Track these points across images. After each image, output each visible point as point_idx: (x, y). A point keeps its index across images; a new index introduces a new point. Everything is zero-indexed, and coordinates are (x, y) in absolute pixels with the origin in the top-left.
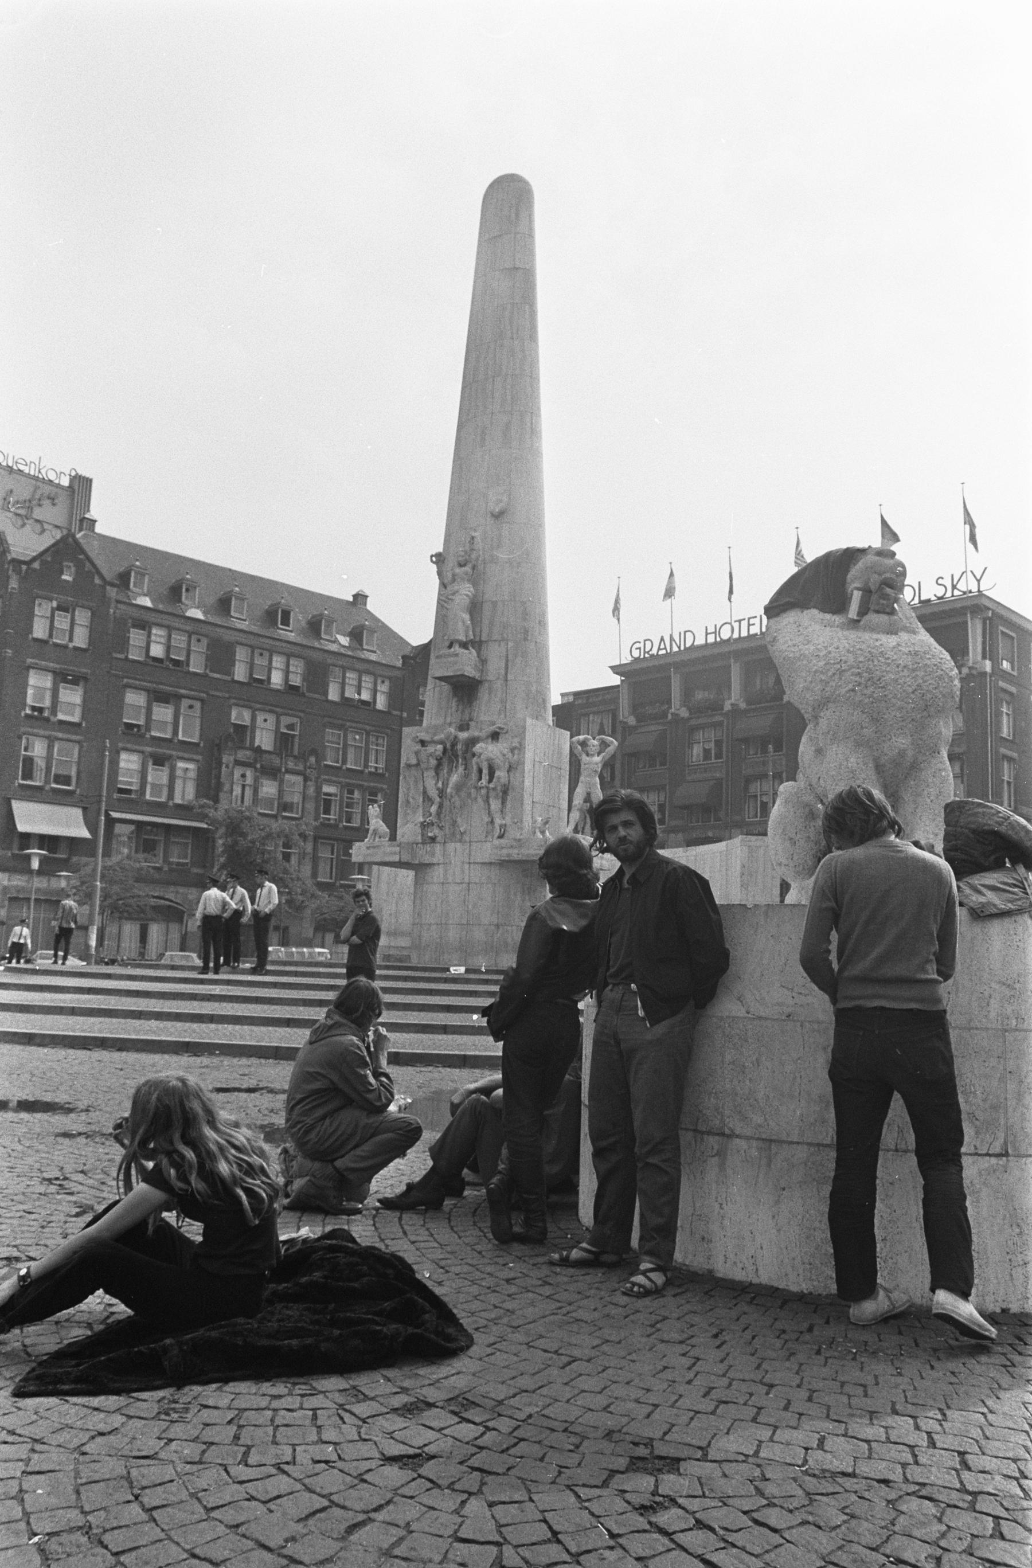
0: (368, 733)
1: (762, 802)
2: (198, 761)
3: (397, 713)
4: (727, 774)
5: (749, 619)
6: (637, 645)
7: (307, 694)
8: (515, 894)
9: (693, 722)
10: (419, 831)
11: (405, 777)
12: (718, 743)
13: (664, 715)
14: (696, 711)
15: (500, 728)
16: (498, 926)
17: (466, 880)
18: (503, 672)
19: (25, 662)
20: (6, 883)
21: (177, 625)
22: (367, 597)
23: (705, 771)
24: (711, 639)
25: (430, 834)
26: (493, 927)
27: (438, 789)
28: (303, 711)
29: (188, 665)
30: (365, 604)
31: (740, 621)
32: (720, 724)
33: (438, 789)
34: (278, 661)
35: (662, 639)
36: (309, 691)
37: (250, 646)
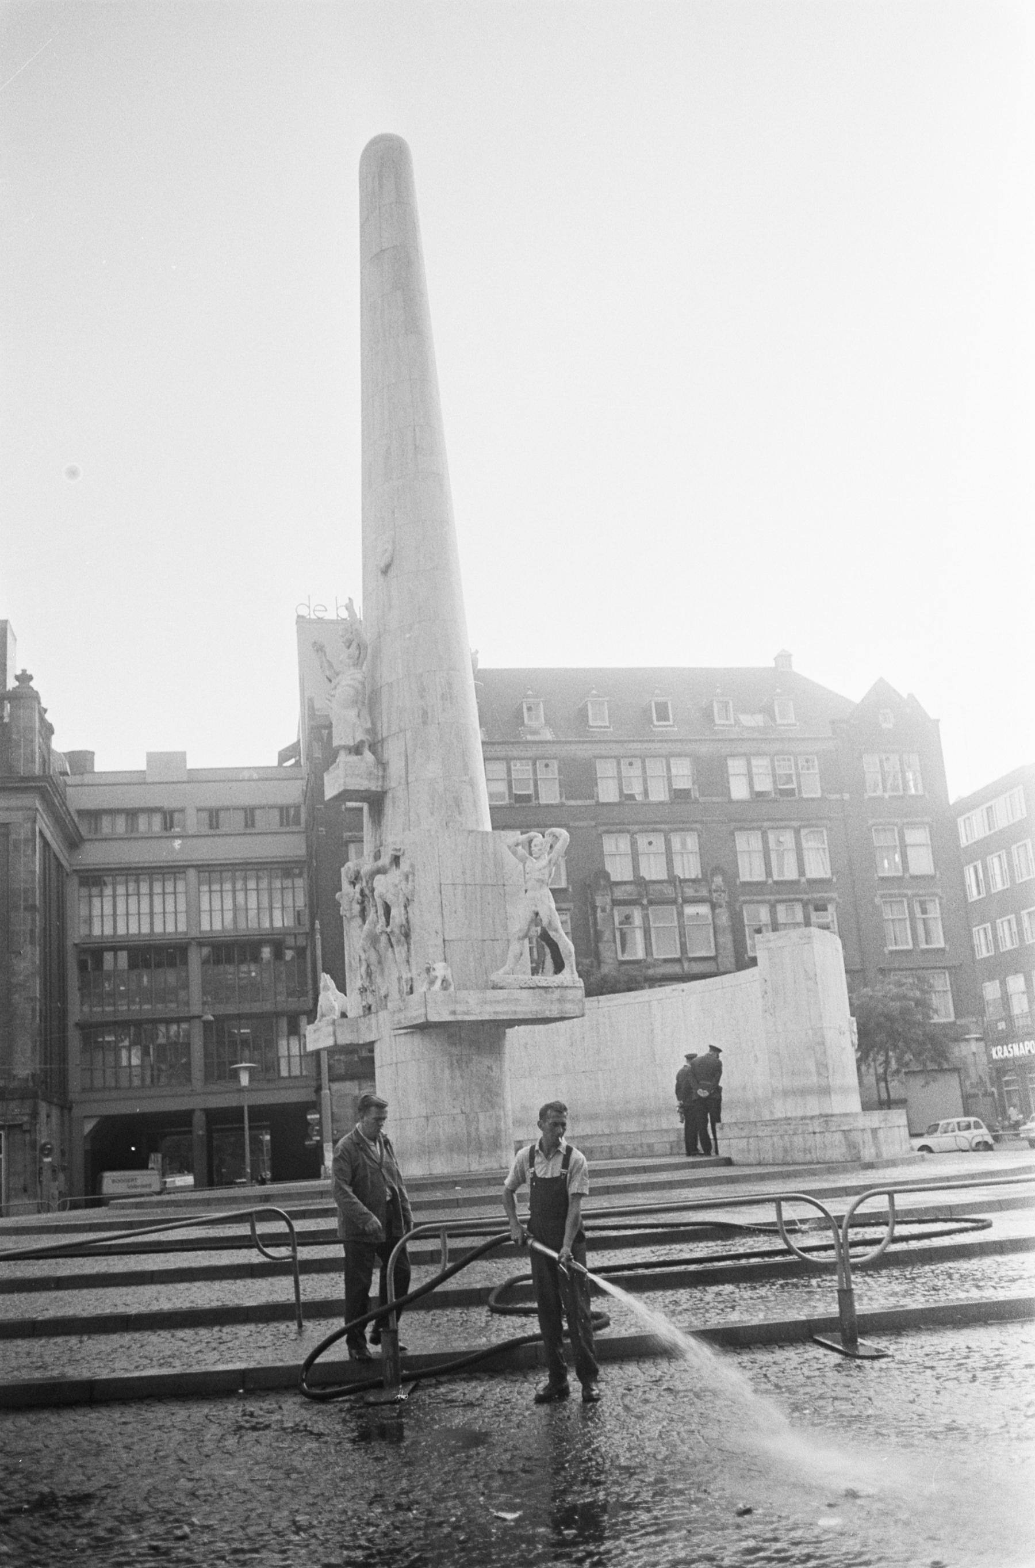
0: (797, 831)
2: (568, 910)
3: (838, 796)
7: (701, 800)
8: (442, 1070)
15: (396, 850)
16: (427, 1118)
18: (403, 772)
19: (342, 838)
20: (357, 1092)
21: (515, 754)
22: (790, 656)
25: (364, 1003)
26: (422, 1119)
28: (701, 822)
29: (537, 798)
30: (790, 666)
34: (655, 768)
36: (702, 795)
37: (615, 757)
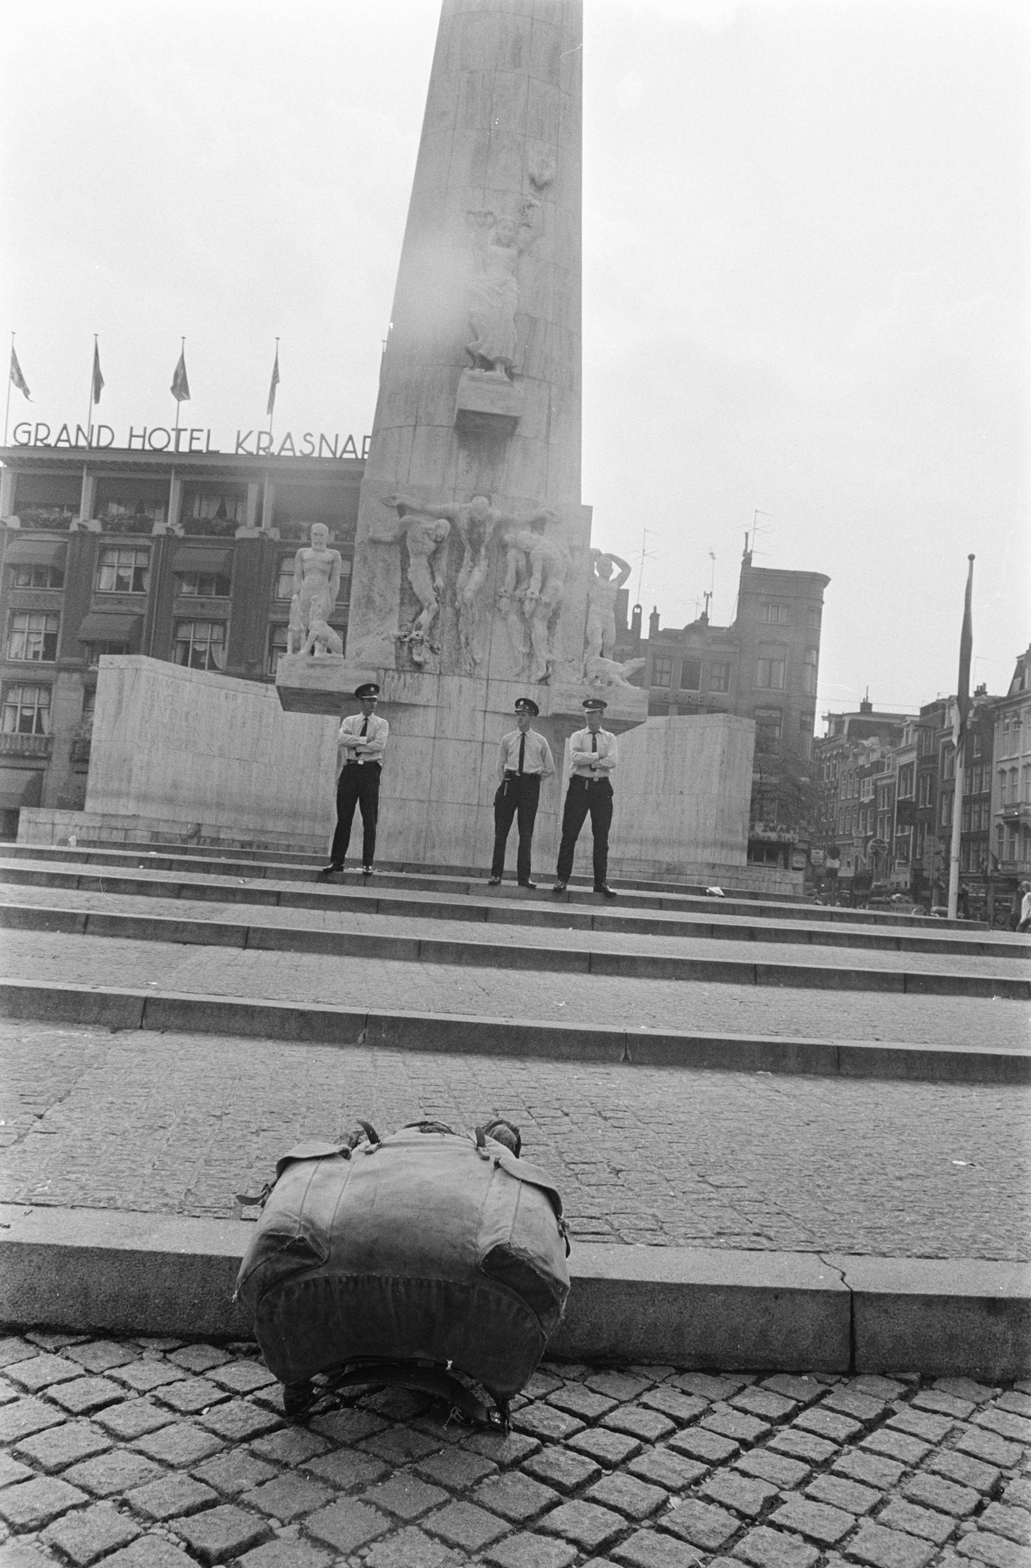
1: (194, 650)
4: (151, 611)
5: (192, 431)
6: (26, 428)
9: (108, 540)
10: (392, 649)
11: (365, 559)
12: (139, 572)
13: (65, 524)
14: (112, 526)
15: (551, 514)
17: (480, 739)
23: (120, 602)
24: (137, 444)
25: (417, 658)
27: (436, 589)
31: (179, 431)
32: (146, 550)
33: (436, 589)
35: (65, 427)
